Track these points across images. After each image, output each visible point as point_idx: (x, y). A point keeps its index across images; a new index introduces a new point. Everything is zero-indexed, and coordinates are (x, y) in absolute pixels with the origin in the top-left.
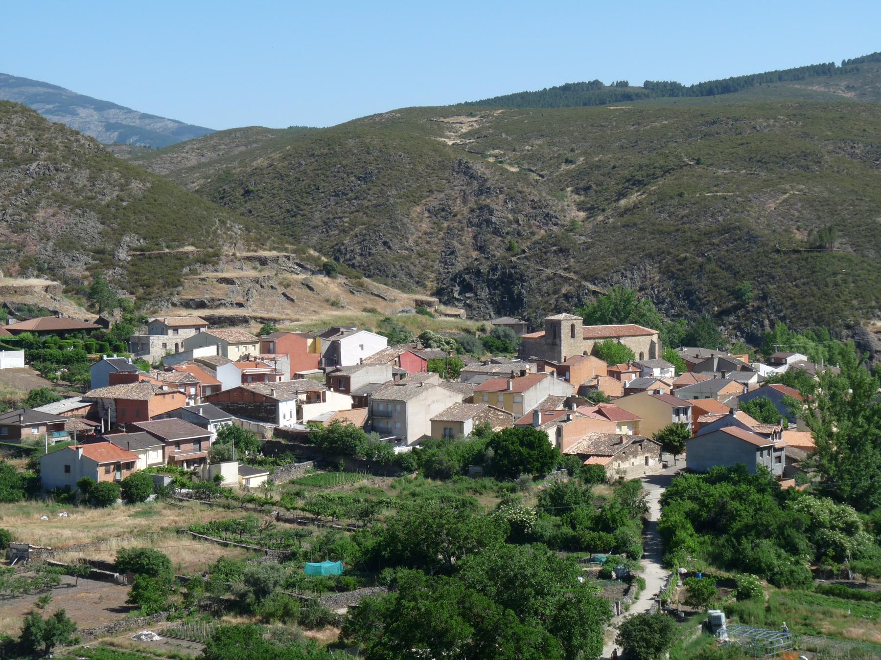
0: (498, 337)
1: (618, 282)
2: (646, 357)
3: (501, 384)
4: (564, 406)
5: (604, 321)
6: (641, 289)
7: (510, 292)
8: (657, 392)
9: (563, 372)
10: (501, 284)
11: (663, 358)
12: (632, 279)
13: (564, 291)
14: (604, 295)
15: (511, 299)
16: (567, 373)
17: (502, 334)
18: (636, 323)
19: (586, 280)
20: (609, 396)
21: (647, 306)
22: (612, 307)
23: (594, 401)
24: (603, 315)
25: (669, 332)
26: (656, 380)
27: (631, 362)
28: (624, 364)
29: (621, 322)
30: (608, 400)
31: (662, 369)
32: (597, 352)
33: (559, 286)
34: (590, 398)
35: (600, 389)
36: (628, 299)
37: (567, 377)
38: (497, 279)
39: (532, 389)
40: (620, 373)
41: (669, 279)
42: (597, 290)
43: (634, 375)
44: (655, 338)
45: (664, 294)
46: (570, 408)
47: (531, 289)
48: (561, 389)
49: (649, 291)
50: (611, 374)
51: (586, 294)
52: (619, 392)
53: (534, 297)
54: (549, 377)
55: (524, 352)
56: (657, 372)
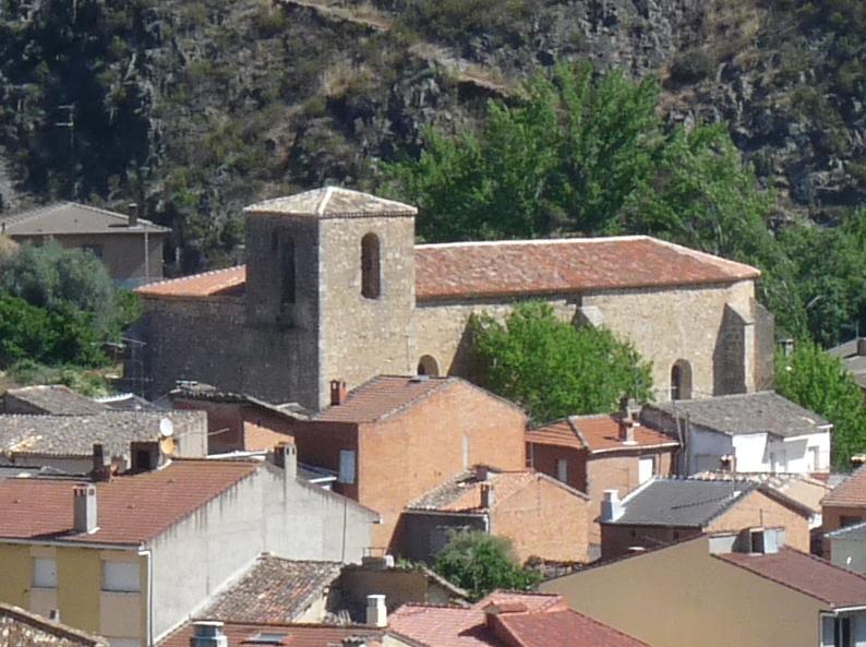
0: (35, 296)
1: (574, 46)
2: (702, 384)
3: (48, 504)
4: (333, 607)
5: (509, 219)
6: (681, 77)
7: (86, 91)
8: (749, 542)
9: (325, 452)
10: (48, 55)
11: (779, 386)
12: (637, 31)
13: (329, 85)
14: (512, 102)
15: (91, 118)
16: (346, 458)
17: (49, 278)
18: (656, 228)
19: (432, 36)
20: (533, 562)
21: (707, 155)
22: (549, 156)
23: (466, 583)
24: (505, 193)
25: (803, 273)
26: (747, 486)
27: (633, 408)
28: (602, 418)
29: (588, 224)
30: (529, 578)
31: (773, 437)
32: (478, 363)
33: (306, 64)
34: (448, 571)
35: (494, 529)
36: (621, 121)
37: (346, 474)
38: (30, 33)
39: (186, 532)
40: (585, 455)
41: (805, 29)
42: (481, 79)
43: (645, 466)
44: (742, 299)
45: (783, 99)
46: (360, 612)
47: (182, 77)
48: (319, 531)
49: (714, 87)
50: (544, 459)
51: (432, 99)
52: (579, 543)
53: (195, 112)
54: (263, 476)
55: (151, 365)
56: (749, 452)
